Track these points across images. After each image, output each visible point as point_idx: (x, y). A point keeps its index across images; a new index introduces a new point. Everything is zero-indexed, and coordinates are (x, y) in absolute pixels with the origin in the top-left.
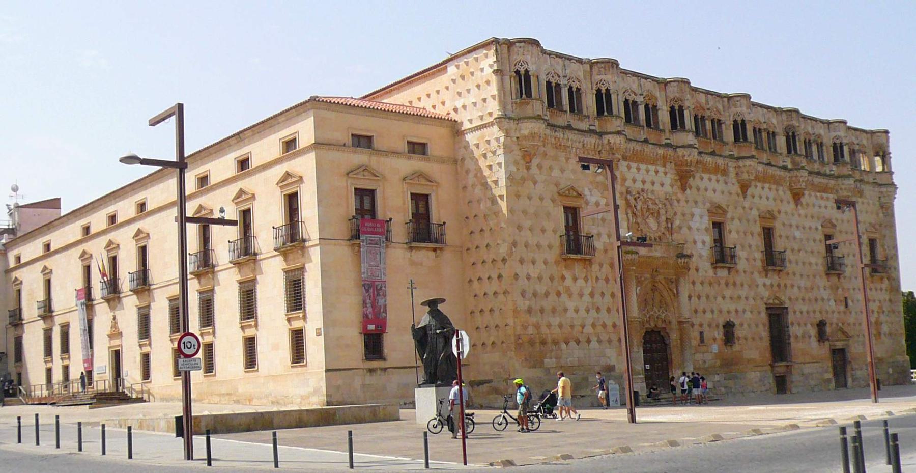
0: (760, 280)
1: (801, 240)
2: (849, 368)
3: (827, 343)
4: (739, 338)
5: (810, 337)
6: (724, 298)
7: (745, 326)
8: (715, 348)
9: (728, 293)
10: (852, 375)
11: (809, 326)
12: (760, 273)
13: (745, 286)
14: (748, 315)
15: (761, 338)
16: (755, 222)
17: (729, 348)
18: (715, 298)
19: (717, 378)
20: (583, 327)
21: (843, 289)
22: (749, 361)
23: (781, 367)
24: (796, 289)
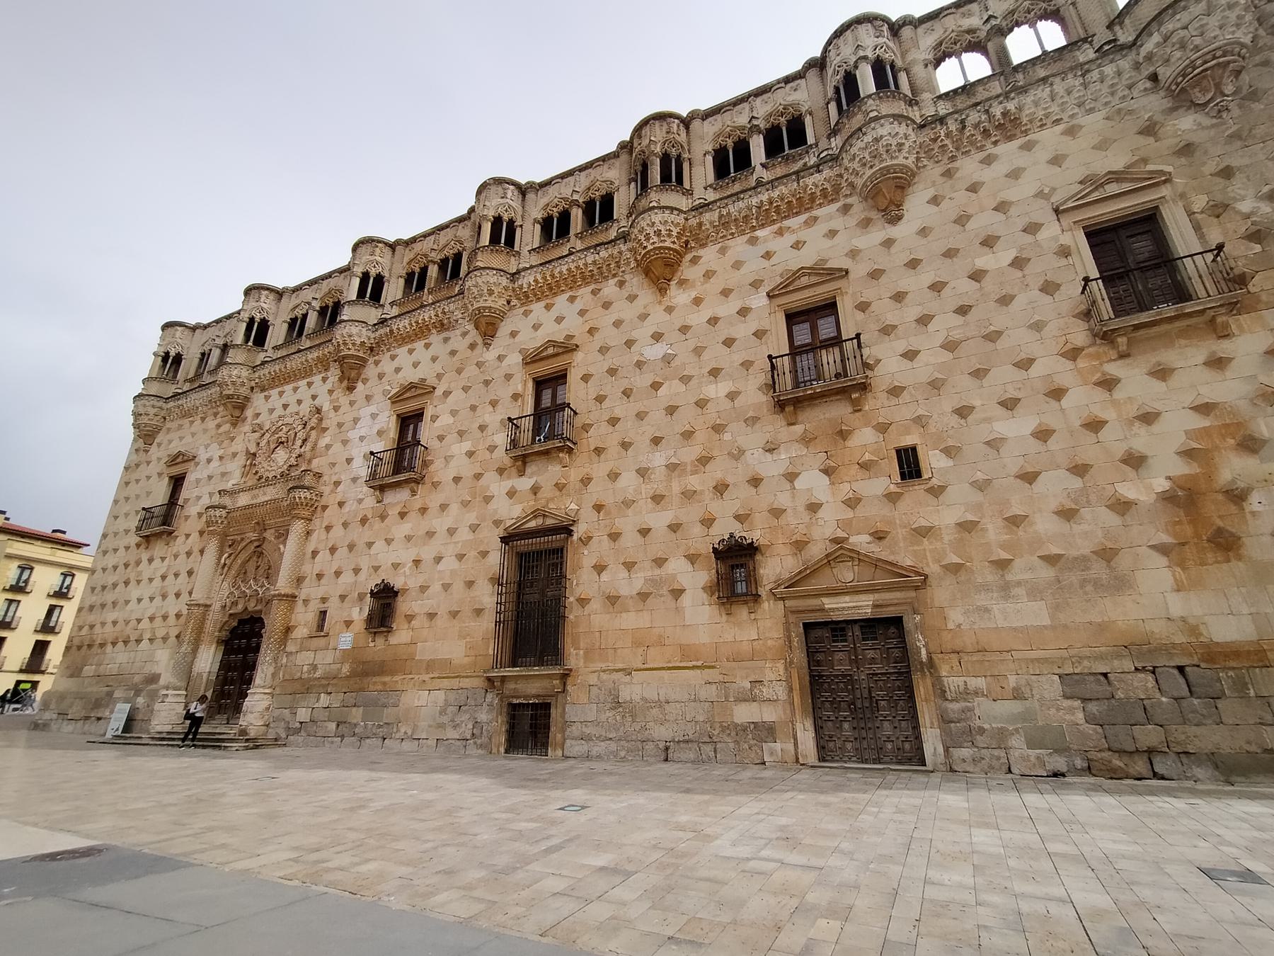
0: (498, 487)
1: (668, 359)
2: (922, 688)
3: (766, 605)
4: (410, 618)
5: (677, 593)
6: (389, 541)
7: (436, 587)
8: (346, 640)
9: (401, 530)
10: (945, 720)
11: (678, 567)
12: (501, 471)
13: (454, 508)
14: (449, 563)
15: (479, 612)
16: (508, 377)
17: (380, 641)
18: (370, 545)
19: (324, 700)
20: (139, 621)
21: (883, 428)
22: (430, 666)
23: (531, 682)
24: (629, 480)
